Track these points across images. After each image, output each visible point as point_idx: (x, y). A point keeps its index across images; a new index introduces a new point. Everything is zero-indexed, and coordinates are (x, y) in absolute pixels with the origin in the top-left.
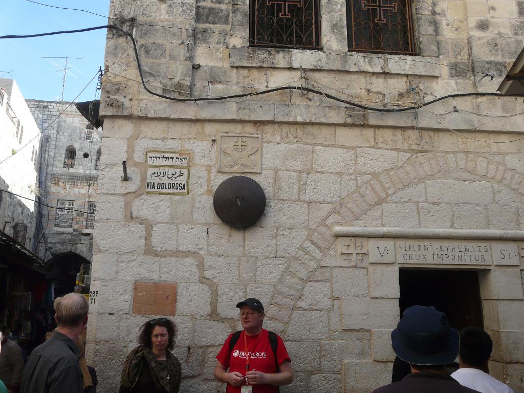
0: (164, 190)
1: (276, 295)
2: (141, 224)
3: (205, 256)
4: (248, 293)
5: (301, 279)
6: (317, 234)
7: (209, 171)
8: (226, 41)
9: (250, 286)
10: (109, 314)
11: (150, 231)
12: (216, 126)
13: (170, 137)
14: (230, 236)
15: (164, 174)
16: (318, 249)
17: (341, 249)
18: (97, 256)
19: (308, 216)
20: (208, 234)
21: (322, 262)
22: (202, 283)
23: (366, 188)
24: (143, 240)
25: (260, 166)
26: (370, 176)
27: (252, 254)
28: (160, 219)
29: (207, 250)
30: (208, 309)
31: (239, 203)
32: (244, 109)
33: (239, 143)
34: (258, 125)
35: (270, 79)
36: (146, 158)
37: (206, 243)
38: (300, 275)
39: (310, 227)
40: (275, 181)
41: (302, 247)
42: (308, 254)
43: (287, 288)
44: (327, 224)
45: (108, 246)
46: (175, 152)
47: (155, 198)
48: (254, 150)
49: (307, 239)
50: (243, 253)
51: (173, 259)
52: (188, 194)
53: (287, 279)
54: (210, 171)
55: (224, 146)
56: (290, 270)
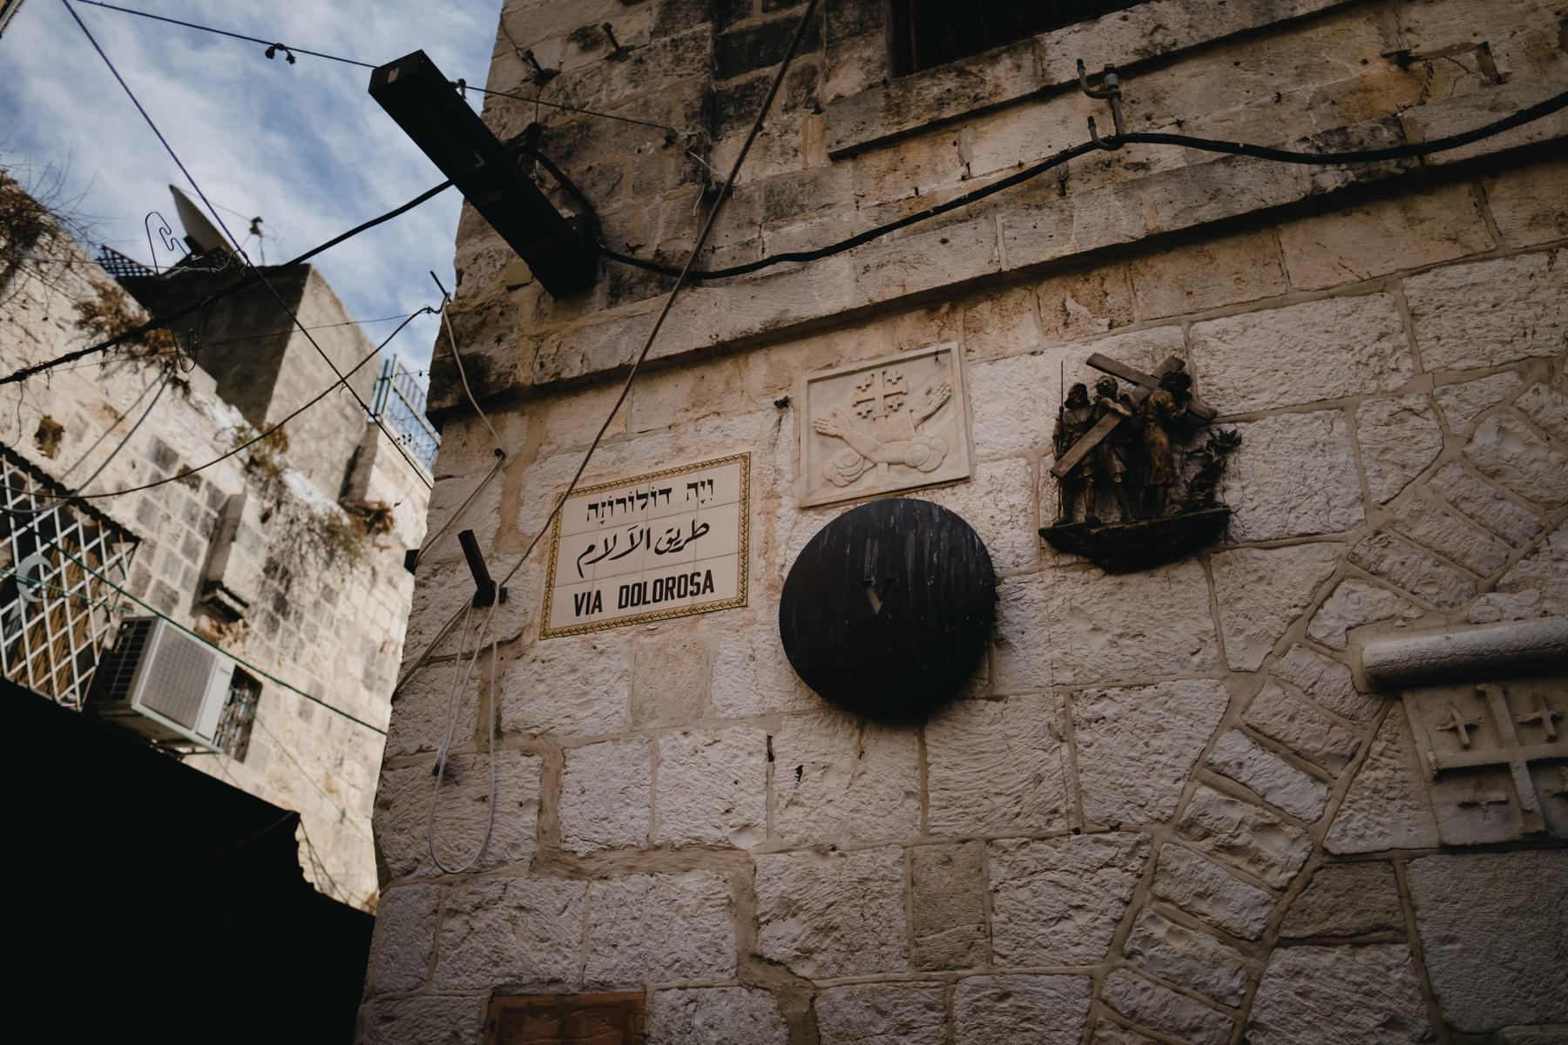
1: (1103, 1034)
2: (527, 753)
4: (960, 1026)
5: (1225, 934)
6: (1277, 691)
8: (815, 95)
9: (965, 986)
11: (558, 772)
12: (792, 356)
13: (637, 428)
14: (861, 754)
16: (1299, 768)
17: (1432, 750)
19: (1211, 614)
20: (771, 757)
21: (1334, 833)
22: (752, 988)
23: (1501, 430)
24: (530, 817)
25: (964, 450)
26: (1510, 377)
27: (962, 828)
28: (591, 726)
29: (769, 831)
31: (877, 606)
32: (880, 266)
33: (877, 391)
34: (944, 310)
35: (975, 151)
37: (763, 798)
38: (1220, 914)
39: (1233, 665)
41: (1210, 765)
42: (1244, 800)
43: (1160, 991)
44: (1319, 635)
45: (412, 854)
48: (936, 400)
49: (1224, 725)
50: (925, 830)
51: (638, 882)
53: (1148, 940)
54: (773, 512)
55: (820, 413)
56: (1160, 888)
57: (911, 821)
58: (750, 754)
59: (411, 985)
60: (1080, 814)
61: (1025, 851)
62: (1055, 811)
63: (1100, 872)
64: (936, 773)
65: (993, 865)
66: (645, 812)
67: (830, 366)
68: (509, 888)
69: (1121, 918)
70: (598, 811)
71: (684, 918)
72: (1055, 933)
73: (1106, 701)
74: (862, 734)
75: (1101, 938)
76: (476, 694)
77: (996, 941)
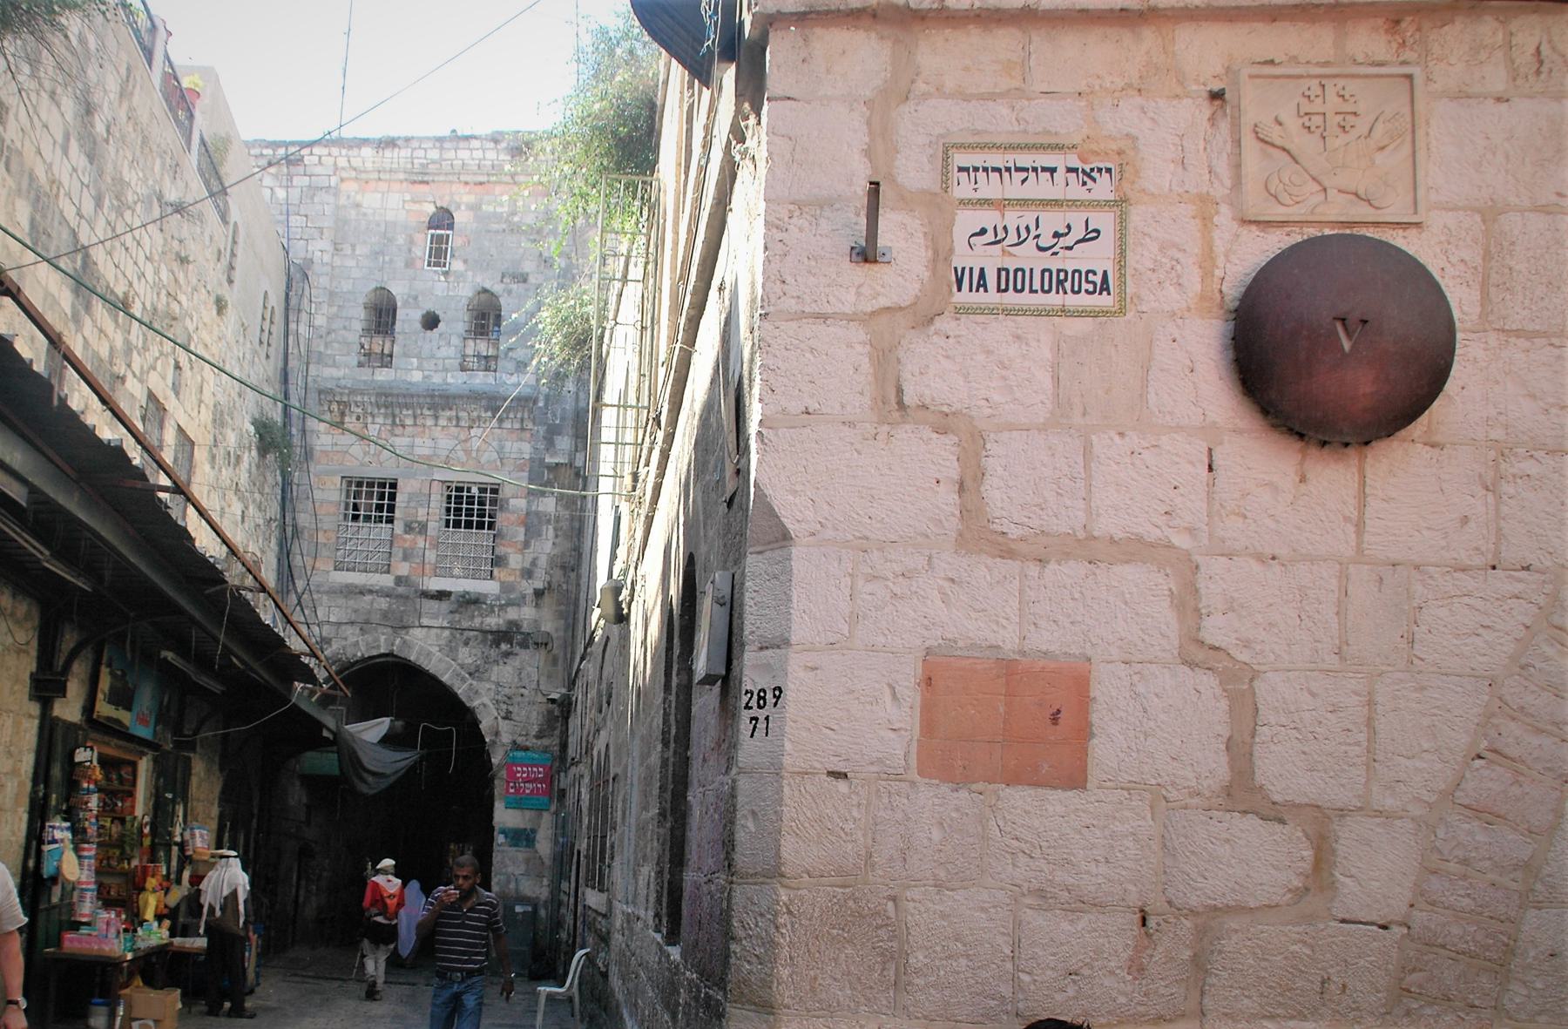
0: (1026, 298)
2: (941, 430)
3: (1199, 559)
4: (1379, 708)
7: (1206, 221)
10: (831, 774)
14: (1303, 479)
15: (1024, 235)
18: (768, 554)
22: (1192, 665)
30: (1216, 768)
36: (945, 172)
40: (1487, 257)
46: (1058, 147)
47: (1001, 329)
50: (1359, 549)
52: (1122, 311)
57: (1347, 542)
58: (1191, 463)
59: (832, 641)
60: (1497, 553)
61: (1447, 578)
62: (1477, 549)
63: (1509, 601)
64: (1373, 505)
65: (1419, 588)
66: (1081, 504)
67: (1272, 62)
68: (935, 560)
69: (1522, 639)
70: (1028, 498)
71: (1126, 603)
72: (1466, 645)
73: (1532, 461)
74: (1304, 457)
75: (1505, 653)
76: (867, 360)
77: (1416, 646)
